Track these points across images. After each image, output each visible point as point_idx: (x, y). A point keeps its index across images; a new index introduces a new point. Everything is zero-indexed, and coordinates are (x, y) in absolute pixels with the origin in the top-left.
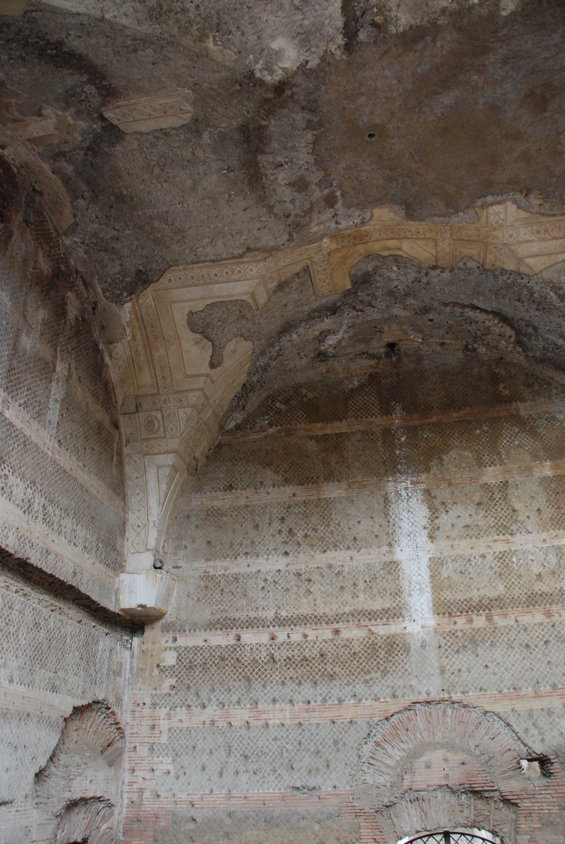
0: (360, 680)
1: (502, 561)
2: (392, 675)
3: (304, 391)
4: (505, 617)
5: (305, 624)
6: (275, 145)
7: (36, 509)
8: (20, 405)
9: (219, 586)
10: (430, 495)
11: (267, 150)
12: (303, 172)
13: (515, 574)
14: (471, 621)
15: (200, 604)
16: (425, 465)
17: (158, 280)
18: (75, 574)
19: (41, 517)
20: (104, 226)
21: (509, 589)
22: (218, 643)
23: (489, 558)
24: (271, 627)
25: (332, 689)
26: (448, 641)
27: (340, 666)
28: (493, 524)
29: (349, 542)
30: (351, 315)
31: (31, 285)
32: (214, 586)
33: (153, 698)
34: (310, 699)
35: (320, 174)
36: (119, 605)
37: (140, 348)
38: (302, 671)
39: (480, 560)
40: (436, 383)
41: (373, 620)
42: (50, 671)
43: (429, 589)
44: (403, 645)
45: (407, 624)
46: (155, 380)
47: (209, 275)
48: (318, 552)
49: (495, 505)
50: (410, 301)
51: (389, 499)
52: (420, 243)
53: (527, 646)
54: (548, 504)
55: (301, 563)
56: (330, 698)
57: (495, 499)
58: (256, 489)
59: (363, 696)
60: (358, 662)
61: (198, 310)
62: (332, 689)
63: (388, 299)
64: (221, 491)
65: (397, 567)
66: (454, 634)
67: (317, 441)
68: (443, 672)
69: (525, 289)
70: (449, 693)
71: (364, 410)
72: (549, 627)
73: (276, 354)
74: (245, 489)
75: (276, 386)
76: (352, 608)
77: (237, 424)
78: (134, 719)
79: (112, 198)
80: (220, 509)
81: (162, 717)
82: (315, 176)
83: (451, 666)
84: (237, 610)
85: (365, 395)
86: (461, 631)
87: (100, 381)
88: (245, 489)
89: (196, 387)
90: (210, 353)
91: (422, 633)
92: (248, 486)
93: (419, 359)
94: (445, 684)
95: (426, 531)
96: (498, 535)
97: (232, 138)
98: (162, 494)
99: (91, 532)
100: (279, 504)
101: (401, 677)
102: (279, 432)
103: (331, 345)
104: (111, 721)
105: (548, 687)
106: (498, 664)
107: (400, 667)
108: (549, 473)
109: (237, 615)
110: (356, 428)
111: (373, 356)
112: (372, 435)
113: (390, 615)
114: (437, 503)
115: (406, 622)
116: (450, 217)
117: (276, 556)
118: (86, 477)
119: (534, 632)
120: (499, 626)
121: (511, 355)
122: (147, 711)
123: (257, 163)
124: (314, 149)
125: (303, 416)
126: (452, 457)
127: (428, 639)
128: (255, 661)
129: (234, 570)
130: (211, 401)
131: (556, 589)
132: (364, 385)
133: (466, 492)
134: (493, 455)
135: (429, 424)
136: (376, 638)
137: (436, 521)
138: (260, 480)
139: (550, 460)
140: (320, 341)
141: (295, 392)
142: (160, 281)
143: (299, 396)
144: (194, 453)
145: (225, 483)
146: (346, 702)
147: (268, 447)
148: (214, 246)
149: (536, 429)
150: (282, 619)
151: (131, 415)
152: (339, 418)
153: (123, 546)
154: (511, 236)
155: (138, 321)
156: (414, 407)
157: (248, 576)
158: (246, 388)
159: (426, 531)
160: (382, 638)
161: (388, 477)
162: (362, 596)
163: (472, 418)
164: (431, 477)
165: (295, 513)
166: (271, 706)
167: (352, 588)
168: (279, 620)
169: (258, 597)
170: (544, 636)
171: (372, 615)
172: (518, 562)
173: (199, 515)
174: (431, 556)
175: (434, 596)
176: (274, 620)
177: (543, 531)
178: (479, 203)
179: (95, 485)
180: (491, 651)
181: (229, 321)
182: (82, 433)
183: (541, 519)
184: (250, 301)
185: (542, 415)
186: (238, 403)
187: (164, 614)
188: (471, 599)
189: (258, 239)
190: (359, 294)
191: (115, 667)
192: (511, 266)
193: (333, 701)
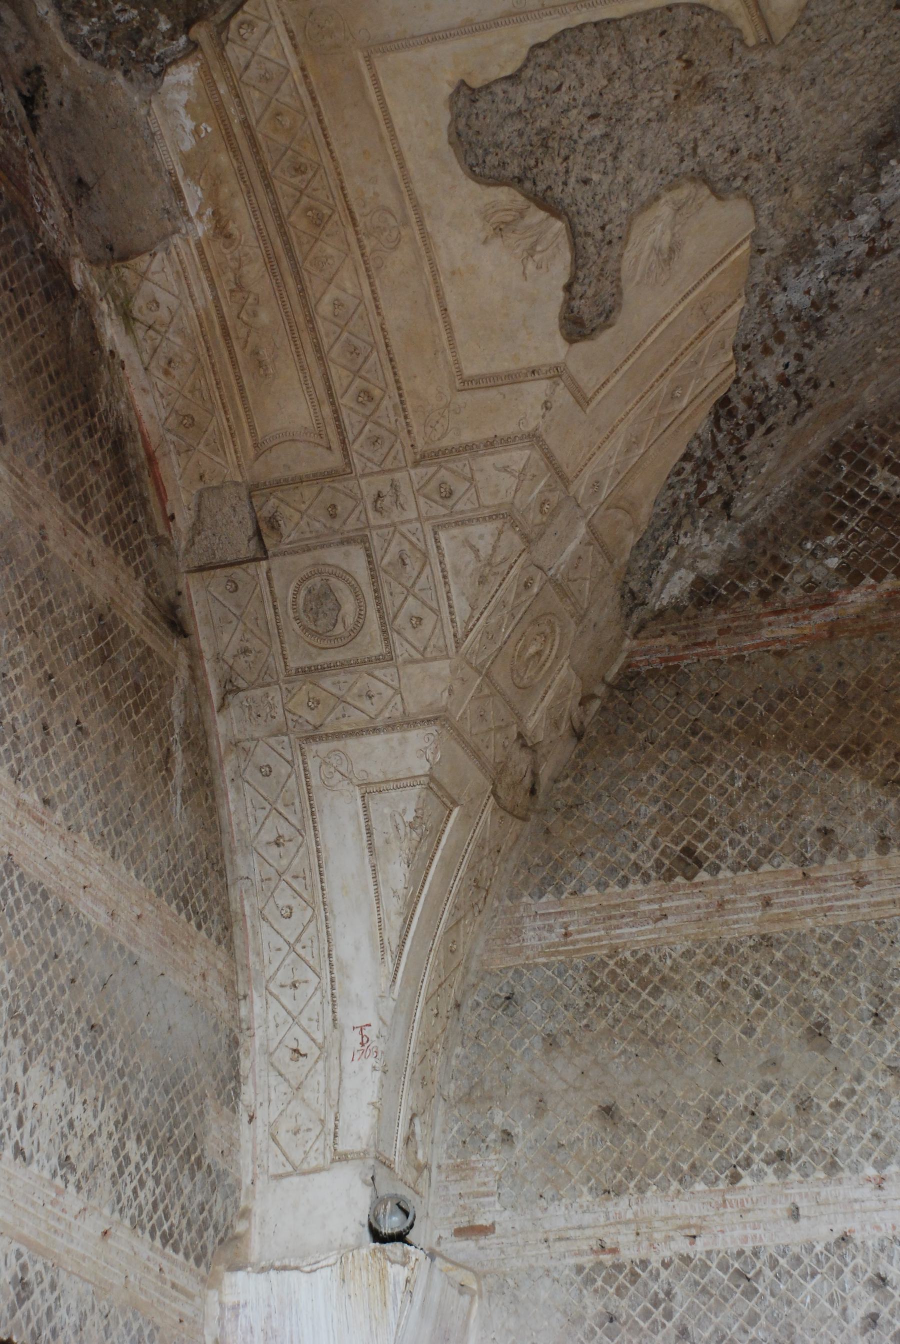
9: (668, 1315)
32: (646, 1315)
37: (255, 272)
46: (327, 410)
58: (802, 861)
64: (646, 879)
73: (864, 247)
74: (754, 866)
75: (869, 398)
77: (700, 581)
80: (646, 959)
87: (91, 431)
88: (754, 866)
89: (510, 428)
90: (560, 270)
92: (765, 852)
98: (393, 906)
99: (90, 1092)
102: (892, 600)
118: (57, 853)
138: (819, 822)
144: (520, 718)
147: (848, 674)
153: (230, 1150)
155: (235, 150)
157: (797, 1264)
158: (731, 414)
173: (558, 992)
179: (98, 885)
181: (639, 114)
182: (27, 662)
186: (701, 485)
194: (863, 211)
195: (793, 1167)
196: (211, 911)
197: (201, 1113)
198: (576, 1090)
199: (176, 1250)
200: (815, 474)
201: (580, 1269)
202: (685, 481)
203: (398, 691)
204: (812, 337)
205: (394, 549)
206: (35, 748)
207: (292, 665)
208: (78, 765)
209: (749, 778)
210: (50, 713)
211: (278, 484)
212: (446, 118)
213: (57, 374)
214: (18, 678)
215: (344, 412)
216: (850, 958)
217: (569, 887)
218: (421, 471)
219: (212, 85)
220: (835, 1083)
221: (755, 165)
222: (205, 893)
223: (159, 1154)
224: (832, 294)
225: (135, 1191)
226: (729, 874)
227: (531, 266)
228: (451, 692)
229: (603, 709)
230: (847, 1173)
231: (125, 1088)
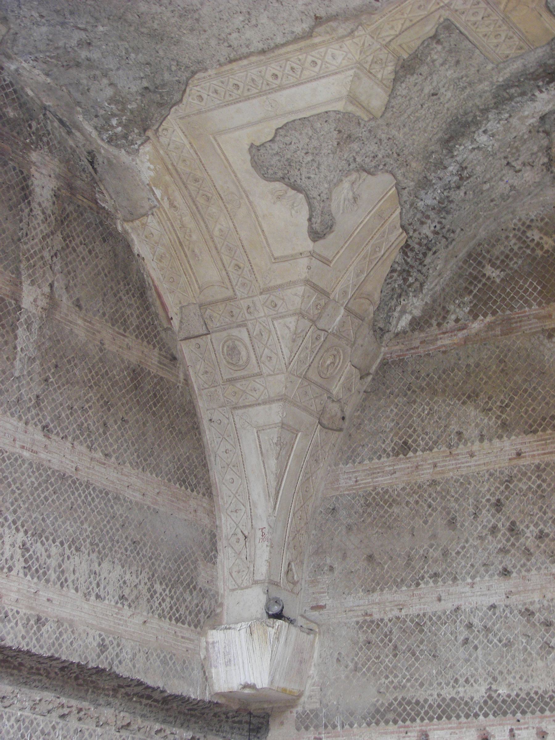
3: (536, 238)
5: (542, 711)
7: (7, 555)
9: (390, 641)
15: (359, 674)
17: (181, 100)
18: (103, 647)
19: (19, 565)
20: (59, 28)
24: (481, 717)
32: (382, 640)
36: (212, 686)
37: (187, 219)
46: (224, 273)
47: (263, 77)
55: (533, 591)
58: (450, 446)
61: (264, 140)
64: (388, 456)
73: (456, 178)
74: (431, 449)
75: (482, 234)
77: (414, 318)
80: (387, 492)
84: (421, 685)
88: (431, 449)
92: (435, 443)
98: (272, 478)
99: (134, 569)
100: (491, 475)
102: (490, 327)
109: (421, 695)
117: (487, 578)
118: (113, 475)
125: (535, 289)
130: (336, 294)
140: (547, 133)
141: (519, 239)
142: (184, 101)
143: (528, 247)
144: (328, 391)
145: (396, 439)
147: (471, 361)
148: (256, 26)
150: (500, 700)
151: (199, 340)
153: (212, 580)
155: (171, 174)
157: (439, 619)
158: (412, 250)
165: (521, 490)
168: (495, 702)
169: (458, 659)
173: (353, 507)
176: (485, 702)
181: (324, 151)
184: (350, 108)
186: (405, 280)
187: (300, 696)
194: (450, 165)
195: (440, 580)
196: (199, 483)
197: (195, 568)
198: (358, 548)
199: (183, 623)
200: (461, 268)
201: (357, 623)
202: (396, 280)
203: (266, 388)
204: (444, 214)
205: (257, 329)
206: (100, 434)
207: (225, 378)
208: (123, 436)
209: (430, 409)
210: (107, 418)
211: (210, 304)
212: (249, 157)
213: (109, 273)
214: (90, 407)
215: (230, 274)
216: (466, 489)
217: (358, 460)
218: (263, 296)
219: (157, 151)
220: (458, 543)
221: (387, 160)
222: (195, 476)
223: (173, 587)
224: (448, 197)
225: (160, 603)
226: (421, 453)
227: (293, 212)
228: (286, 388)
229: (373, 379)
230: (460, 582)
231: (153, 564)
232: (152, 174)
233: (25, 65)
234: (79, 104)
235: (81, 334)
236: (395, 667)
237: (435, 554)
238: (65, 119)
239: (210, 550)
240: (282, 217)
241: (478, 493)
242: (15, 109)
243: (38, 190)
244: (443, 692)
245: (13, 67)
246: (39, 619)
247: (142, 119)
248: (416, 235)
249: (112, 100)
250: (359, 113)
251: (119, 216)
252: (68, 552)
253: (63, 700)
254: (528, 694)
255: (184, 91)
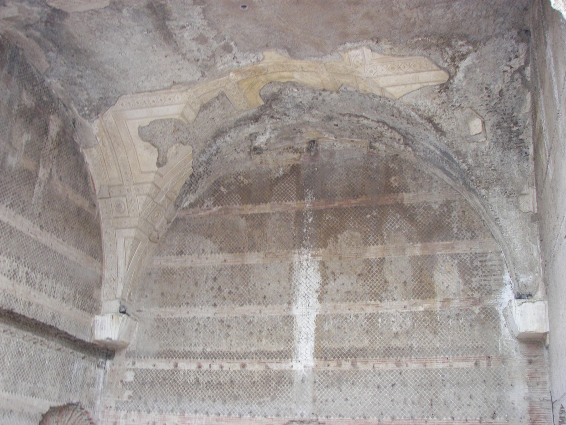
0: (256, 401)
1: (370, 320)
2: (278, 400)
3: (242, 179)
4: (365, 364)
5: (223, 358)
6: (175, 15)
7: (20, 275)
8: (7, 206)
10: (324, 266)
11: (171, 18)
12: (201, 31)
13: (378, 332)
14: (339, 365)
16: (324, 241)
18: (53, 317)
19: (24, 280)
20: (71, 69)
21: (372, 343)
22: (162, 368)
23: (361, 317)
25: (236, 406)
26: (322, 378)
27: (243, 391)
28: (368, 291)
29: (260, 299)
30: (271, 122)
31: (15, 119)
33: (116, 403)
34: (220, 412)
35: (214, 33)
37: (109, 151)
38: (217, 392)
39: (354, 318)
40: (342, 174)
41: (270, 359)
42: (31, 383)
43: (313, 339)
44: (289, 378)
45: (294, 363)
48: (237, 305)
49: (372, 276)
50: (314, 112)
51: (294, 267)
52: (309, 73)
53: (378, 387)
54: (413, 278)
56: (234, 412)
57: (372, 272)
58: (199, 254)
59: (257, 413)
60: (256, 388)
62: (236, 406)
63: (297, 110)
65: (292, 321)
66: (326, 373)
67: (247, 219)
68: (314, 401)
69: (394, 109)
70: (317, 416)
71: (284, 195)
72: (397, 374)
73: (215, 152)
74: (191, 254)
75: (221, 174)
76: (256, 349)
78: (103, 417)
79: (72, 51)
81: (122, 417)
82: (211, 34)
83: (321, 397)
84: (177, 345)
85: (287, 182)
86: (332, 371)
90: (156, 156)
91: (303, 371)
92: (193, 252)
93: (332, 154)
94: (315, 410)
95: (317, 294)
96: (371, 300)
97: (143, 12)
100: (214, 267)
101: (284, 402)
102: (220, 210)
103: (262, 143)
104: (85, 417)
105: (389, 418)
106: (355, 398)
107: (284, 395)
108: (418, 253)
109: (176, 348)
110: (277, 209)
111: (296, 151)
112: (287, 216)
113: (282, 356)
114: (328, 272)
115: (293, 362)
116: (322, 57)
119: (385, 376)
120: (360, 370)
121: (404, 153)
122: (112, 412)
123: (167, 27)
124: (205, 16)
126: (345, 236)
127: (307, 375)
128: (186, 382)
129: (177, 316)
130: (163, 189)
131: (407, 345)
132: (287, 175)
133: (352, 265)
134: (377, 236)
135: (332, 209)
136: (270, 372)
137: (326, 287)
139: (421, 242)
140: (251, 141)
141: (235, 178)
144: (154, 227)
146: (245, 416)
147: (211, 223)
149: (414, 216)
151: (106, 200)
152: (265, 201)
153: (99, 295)
154: (371, 71)
155: (104, 131)
156: (321, 195)
157: (187, 320)
158: (194, 176)
159: (317, 294)
160: (274, 372)
161: (295, 249)
162: (264, 340)
163: (365, 205)
164: (327, 251)
166: (194, 415)
167: (258, 334)
168: (205, 354)
170: (392, 380)
171: (270, 355)
172: (382, 322)
174: (318, 313)
175: (316, 344)
176: (201, 354)
177: (405, 299)
178: (341, 48)
180: (351, 388)
181: (168, 133)
183: (406, 290)
184: (181, 118)
185: (421, 204)
186: (190, 188)
188: (343, 348)
189: (180, 76)
190: (274, 107)
191: (89, 381)
192: (378, 93)
193: (236, 415)
232: (97, 131)
233: (54, 81)
234: (73, 99)
235: (60, 190)
236: (168, 337)
237: (188, 295)
238: (66, 105)
239: (99, 284)
240: (147, 157)
241: (208, 273)
242: (47, 97)
243: (51, 131)
244: (185, 349)
245: (49, 81)
246: (29, 303)
247: (97, 109)
248: (197, 171)
249: (86, 100)
250: (184, 121)
251: (81, 146)
252: (44, 277)
253: (36, 336)
254: (218, 352)
255: (117, 101)
